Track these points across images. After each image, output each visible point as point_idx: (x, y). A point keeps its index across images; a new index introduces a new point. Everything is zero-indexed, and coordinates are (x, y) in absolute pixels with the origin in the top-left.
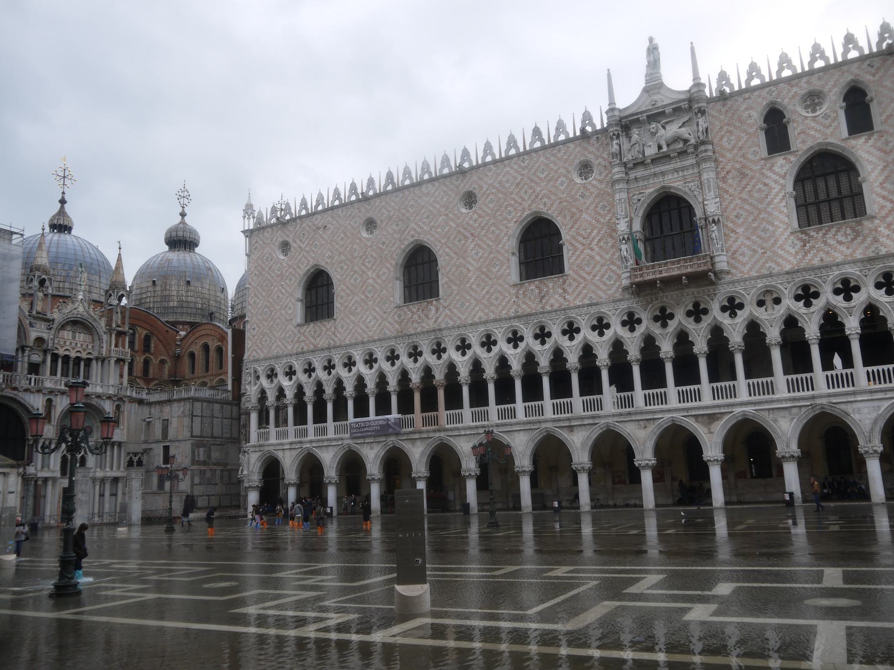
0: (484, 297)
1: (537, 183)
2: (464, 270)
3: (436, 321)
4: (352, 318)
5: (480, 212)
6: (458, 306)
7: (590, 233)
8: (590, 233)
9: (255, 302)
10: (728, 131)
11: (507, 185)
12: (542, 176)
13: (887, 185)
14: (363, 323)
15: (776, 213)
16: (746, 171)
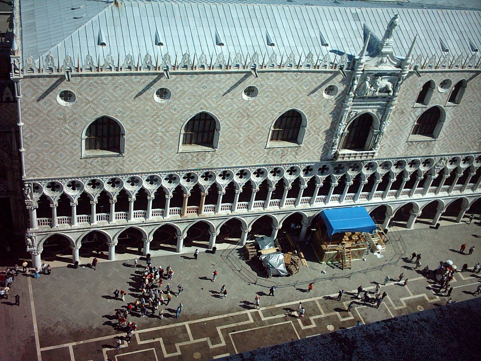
0: (246, 152)
1: (300, 92)
2: (237, 135)
3: (210, 163)
4: (140, 156)
5: (257, 102)
6: (228, 155)
7: (321, 127)
8: (321, 127)
9: (31, 137)
10: (407, 90)
11: (281, 89)
12: (305, 88)
13: (448, 129)
14: (150, 160)
15: (406, 132)
16: (404, 111)
